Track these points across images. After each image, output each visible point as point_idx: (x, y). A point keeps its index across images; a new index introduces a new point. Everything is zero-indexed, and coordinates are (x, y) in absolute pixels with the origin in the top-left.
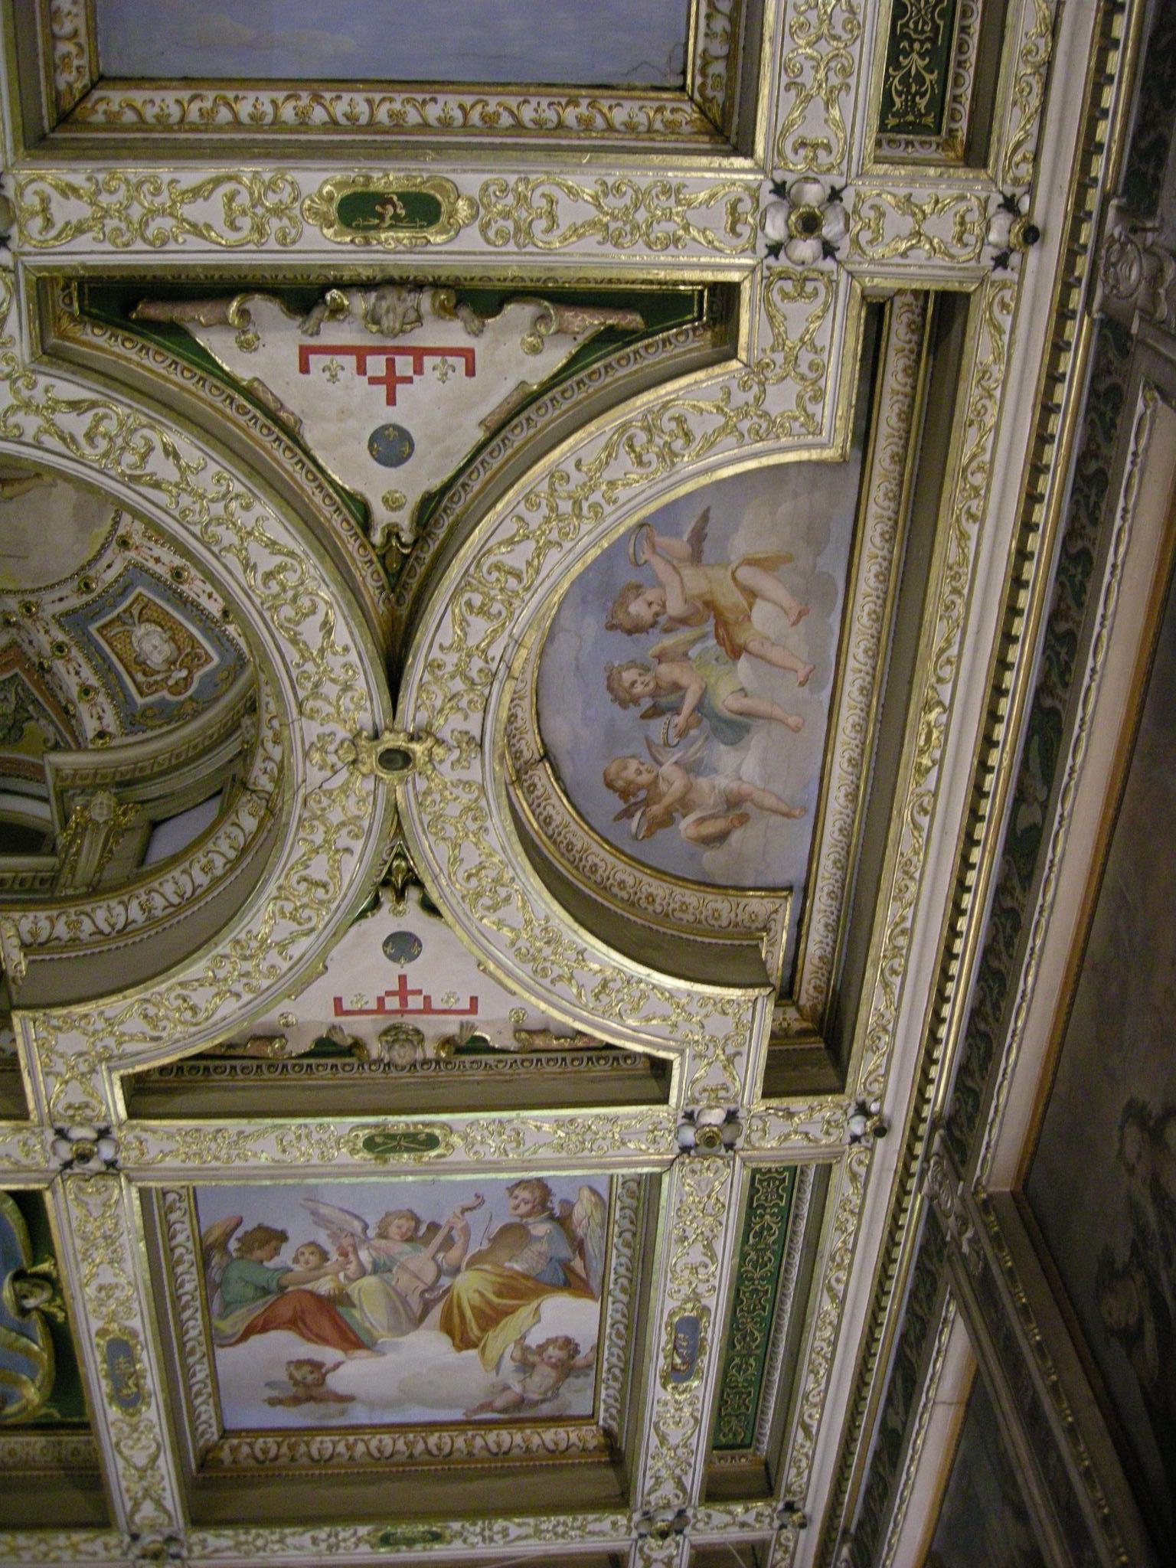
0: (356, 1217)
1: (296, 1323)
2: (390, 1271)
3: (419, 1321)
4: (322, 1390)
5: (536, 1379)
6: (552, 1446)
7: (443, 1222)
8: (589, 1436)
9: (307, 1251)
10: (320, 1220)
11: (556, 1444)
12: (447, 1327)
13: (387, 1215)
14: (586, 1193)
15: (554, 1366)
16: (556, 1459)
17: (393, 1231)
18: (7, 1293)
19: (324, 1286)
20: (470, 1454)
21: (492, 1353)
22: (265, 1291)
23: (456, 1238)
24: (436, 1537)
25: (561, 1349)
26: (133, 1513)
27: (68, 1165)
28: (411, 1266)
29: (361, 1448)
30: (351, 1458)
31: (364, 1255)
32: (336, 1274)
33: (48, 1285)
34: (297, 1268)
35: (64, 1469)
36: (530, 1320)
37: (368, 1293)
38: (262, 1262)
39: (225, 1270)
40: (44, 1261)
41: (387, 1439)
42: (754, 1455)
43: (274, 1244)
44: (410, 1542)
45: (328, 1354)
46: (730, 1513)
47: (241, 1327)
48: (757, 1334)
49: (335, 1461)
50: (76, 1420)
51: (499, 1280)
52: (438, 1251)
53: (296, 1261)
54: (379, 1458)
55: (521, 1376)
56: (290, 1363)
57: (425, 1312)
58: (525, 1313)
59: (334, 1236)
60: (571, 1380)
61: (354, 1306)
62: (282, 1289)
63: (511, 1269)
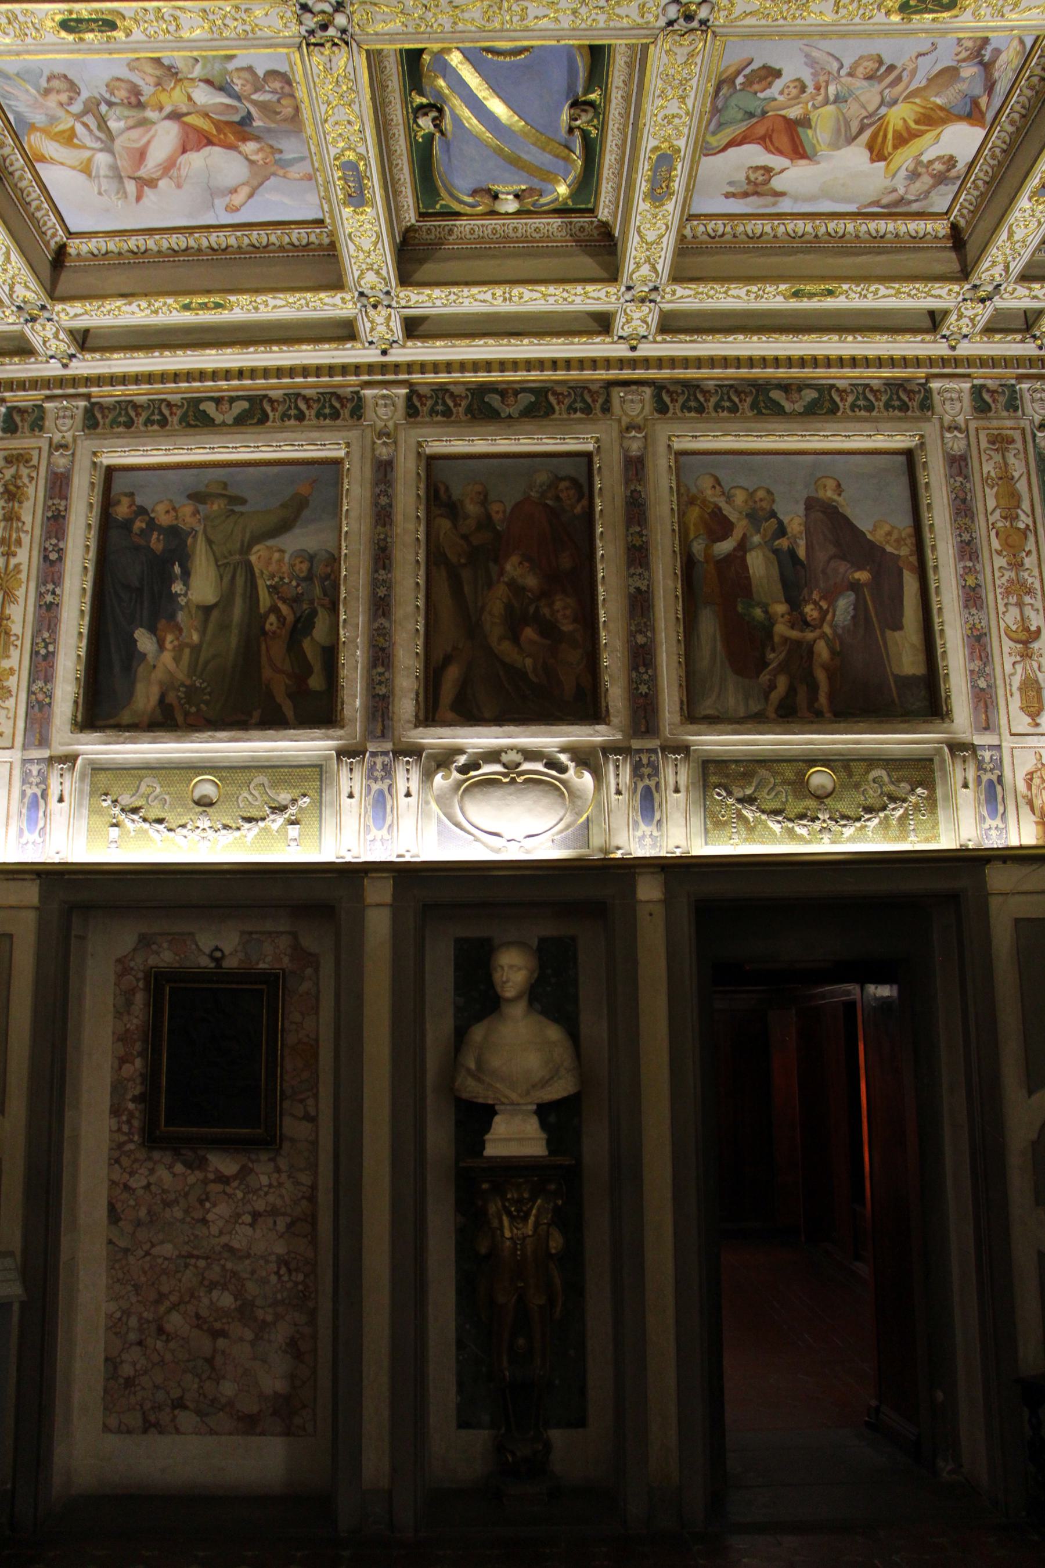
1: (765, 140)
3: (852, 139)
4: (766, 187)
5: (918, 184)
6: (914, 234)
8: (941, 228)
9: (792, 85)
11: (917, 232)
12: (870, 147)
15: (933, 176)
16: (916, 244)
18: (565, 117)
20: (857, 237)
21: (893, 166)
22: (751, 115)
24: (830, 293)
25: (944, 163)
26: (633, 272)
27: (670, 23)
28: (863, 99)
29: (782, 229)
30: (775, 236)
31: (832, 90)
32: (807, 104)
33: (591, 110)
34: (781, 98)
37: (824, 120)
38: (756, 93)
39: (727, 99)
40: (593, 92)
41: (800, 223)
43: (769, 79)
44: (811, 295)
46: (1030, 289)
49: (764, 238)
50: (583, 206)
51: (921, 110)
53: (781, 93)
54: (793, 237)
55: (906, 183)
57: (861, 131)
58: (929, 136)
59: (815, 75)
61: (810, 127)
62: (764, 113)
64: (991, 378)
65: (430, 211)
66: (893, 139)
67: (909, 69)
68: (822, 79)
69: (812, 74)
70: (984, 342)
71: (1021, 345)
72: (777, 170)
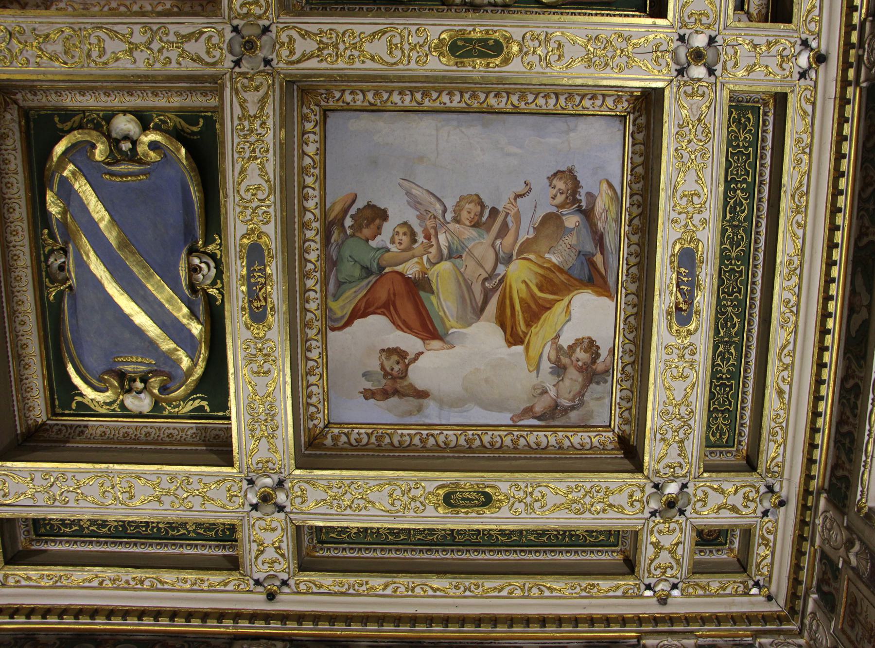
0: (439, 200)
1: (387, 308)
2: (461, 257)
5: (567, 382)
7: (501, 209)
9: (401, 230)
10: (415, 203)
13: (462, 198)
14: (605, 186)
15: (580, 370)
17: (464, 215)
19: (411, 269)
22: (367, 271)
23: (510, 225)
34: (393, 248)
35: (206, 446)
36: (563, 318)
38: (367, 241)
42: (738, 450)
43: (378, 221)
45: (409, 342)
47: (348, 310)
48: (735, 320)
52: (496, 239)
53: (393, 241)
56: (383, 350)
58: (559, 307)
60: (593, 386)
61: (433, 293)
62: (381, 268)
63: (550, 261)
64: (720, 637)
65: (67, 412)
66: (523, 313)
67: (512, 213)
68: (430, 224)
69: (418, 217)
70: (699, 596)
71: (745, 599)
72: (411, 356)
